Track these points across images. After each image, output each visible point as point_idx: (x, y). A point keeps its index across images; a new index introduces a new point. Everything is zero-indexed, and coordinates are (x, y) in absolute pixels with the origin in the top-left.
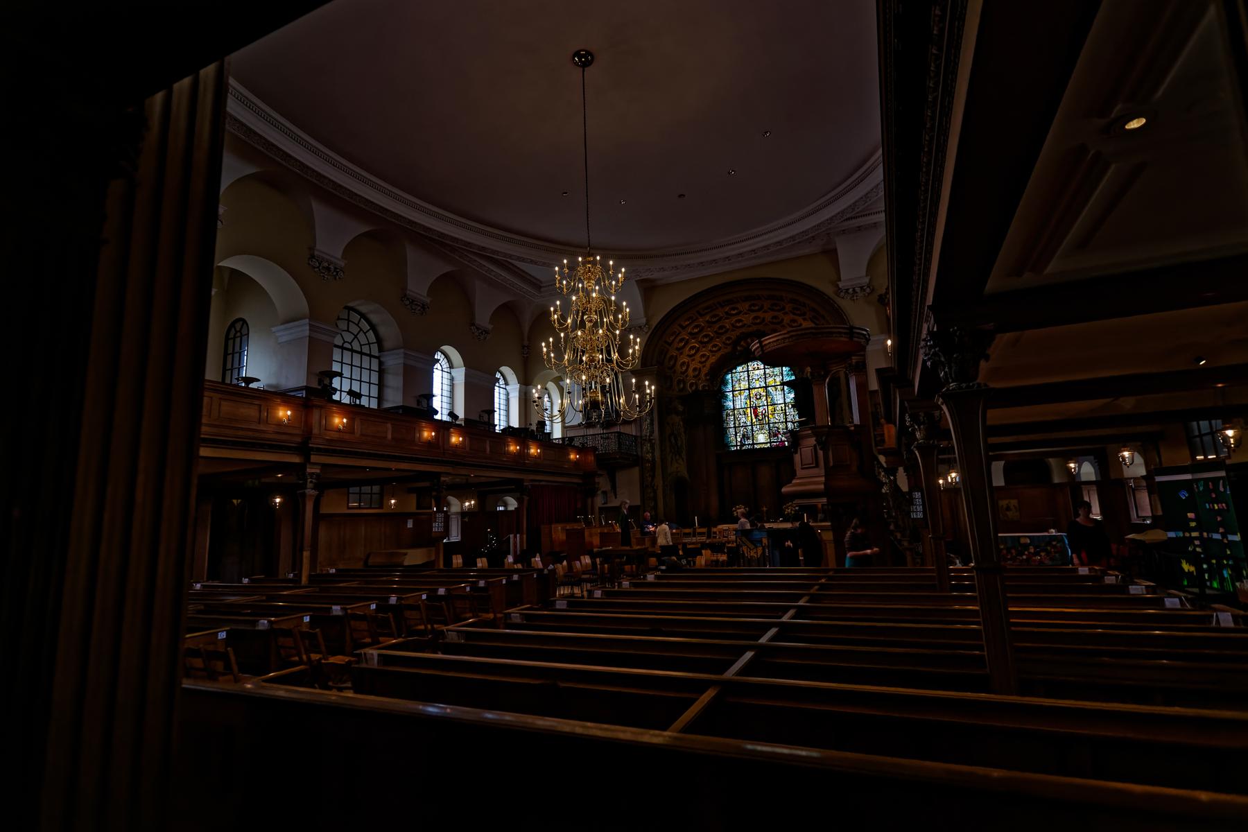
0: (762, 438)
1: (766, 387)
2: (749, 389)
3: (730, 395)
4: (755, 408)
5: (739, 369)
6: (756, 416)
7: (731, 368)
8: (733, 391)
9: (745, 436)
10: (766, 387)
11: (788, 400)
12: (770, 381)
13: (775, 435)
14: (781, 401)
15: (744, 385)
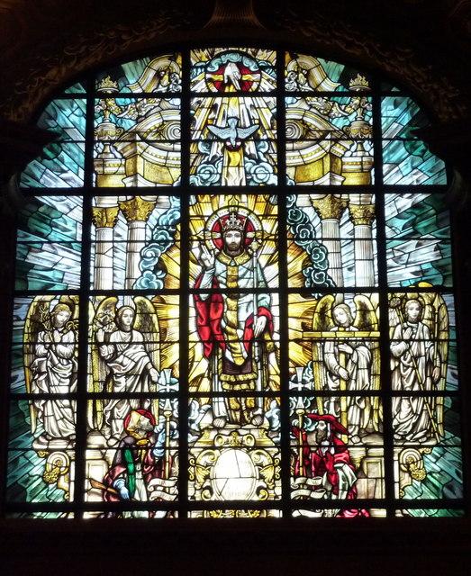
0: (235, 475)
1: (282, 191)
2: (184, 191)
3: (70, 212)
4: (215, 297)
5: (139, 77)
6: (214, 343)
7: (92, 73)
8: (89, 191)
9: (130, 453)
10: (282, 191)
11: (401, 275)
12: (307, 160)
13: (321, 466)
14: (363, 274)
15: (157, 165)
